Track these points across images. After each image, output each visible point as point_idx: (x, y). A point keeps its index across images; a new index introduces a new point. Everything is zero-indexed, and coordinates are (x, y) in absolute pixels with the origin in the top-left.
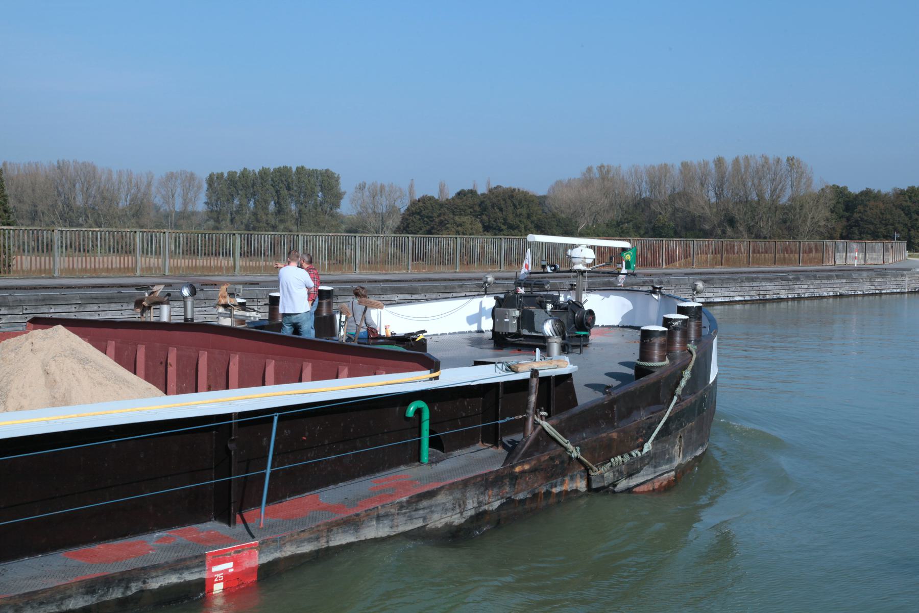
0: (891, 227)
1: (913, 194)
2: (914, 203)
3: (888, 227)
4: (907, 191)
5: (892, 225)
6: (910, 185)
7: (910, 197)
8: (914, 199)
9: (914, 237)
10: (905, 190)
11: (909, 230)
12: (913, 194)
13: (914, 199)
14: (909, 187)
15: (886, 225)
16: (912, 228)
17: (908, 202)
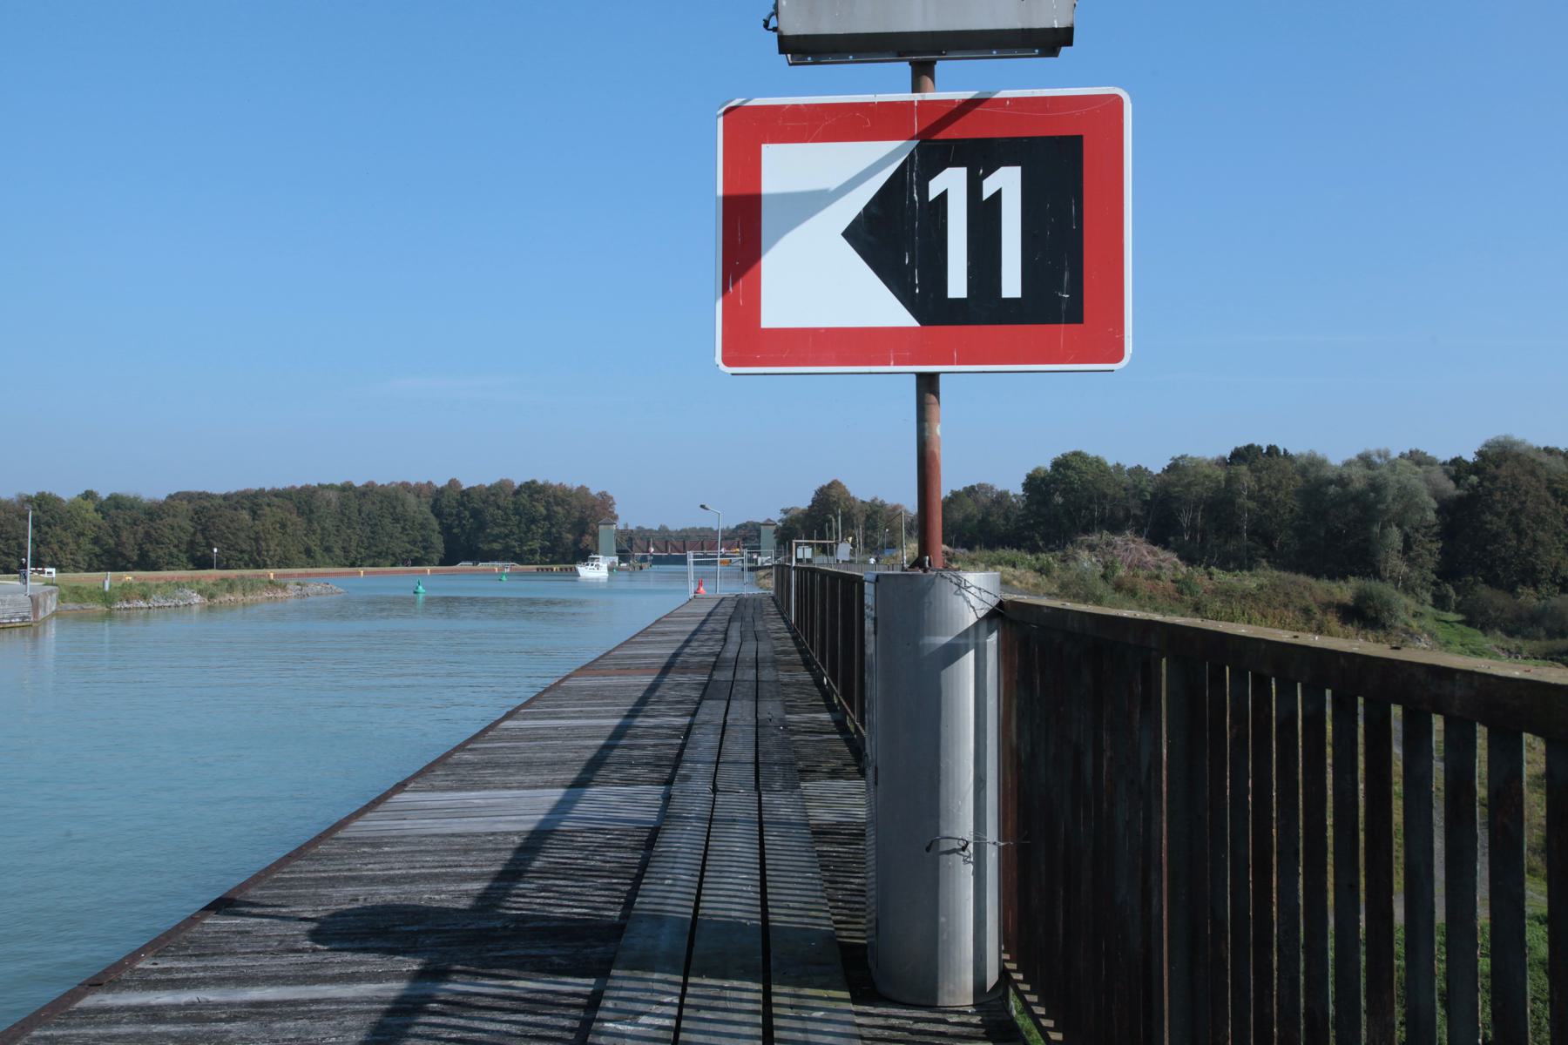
0: (13, 543)
1: (43, 502)
2: (44, 512)
3: (10, 541)
4: (36, 498)
5: (15, 539)
6: (40, 491)
7: (39, 506)
8: (45, 508)
9: (44, 555)
10: (34, 496)
11: (38, 546)
12: (43, 502)
13: (45, 508)
14: (38, 493)
15: (7, 539)
16: (41, 542)
17: (38, 511)
